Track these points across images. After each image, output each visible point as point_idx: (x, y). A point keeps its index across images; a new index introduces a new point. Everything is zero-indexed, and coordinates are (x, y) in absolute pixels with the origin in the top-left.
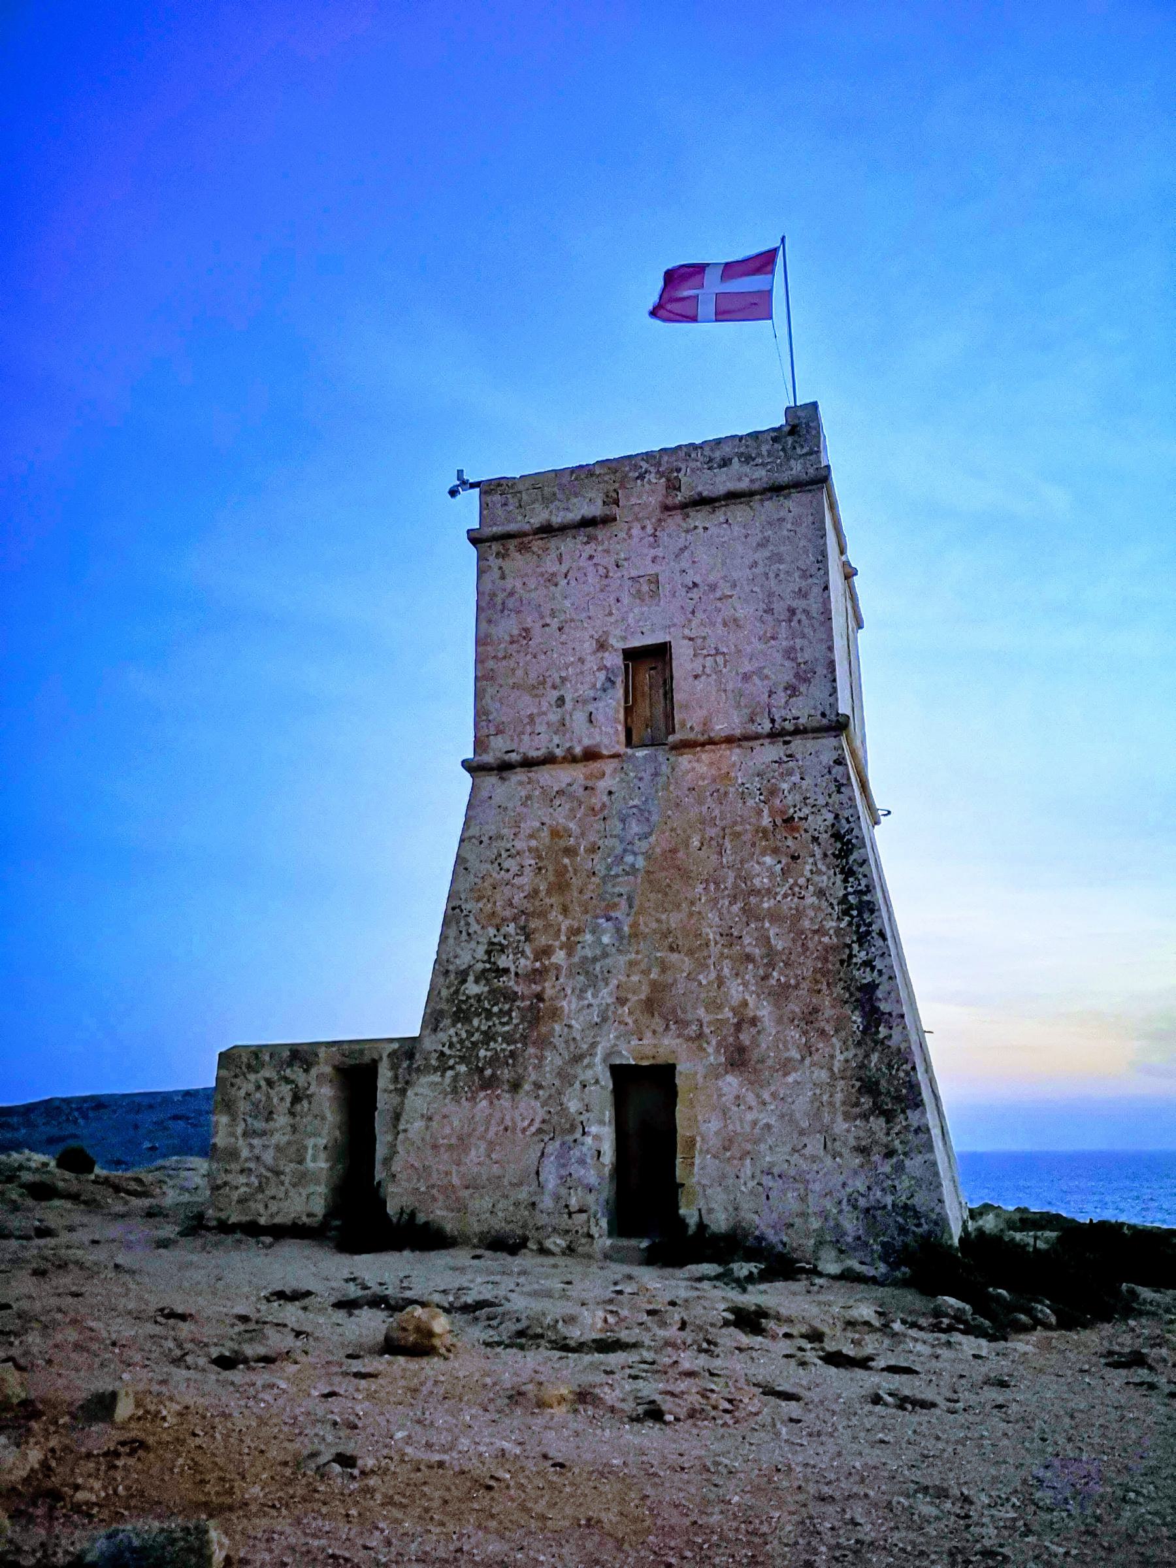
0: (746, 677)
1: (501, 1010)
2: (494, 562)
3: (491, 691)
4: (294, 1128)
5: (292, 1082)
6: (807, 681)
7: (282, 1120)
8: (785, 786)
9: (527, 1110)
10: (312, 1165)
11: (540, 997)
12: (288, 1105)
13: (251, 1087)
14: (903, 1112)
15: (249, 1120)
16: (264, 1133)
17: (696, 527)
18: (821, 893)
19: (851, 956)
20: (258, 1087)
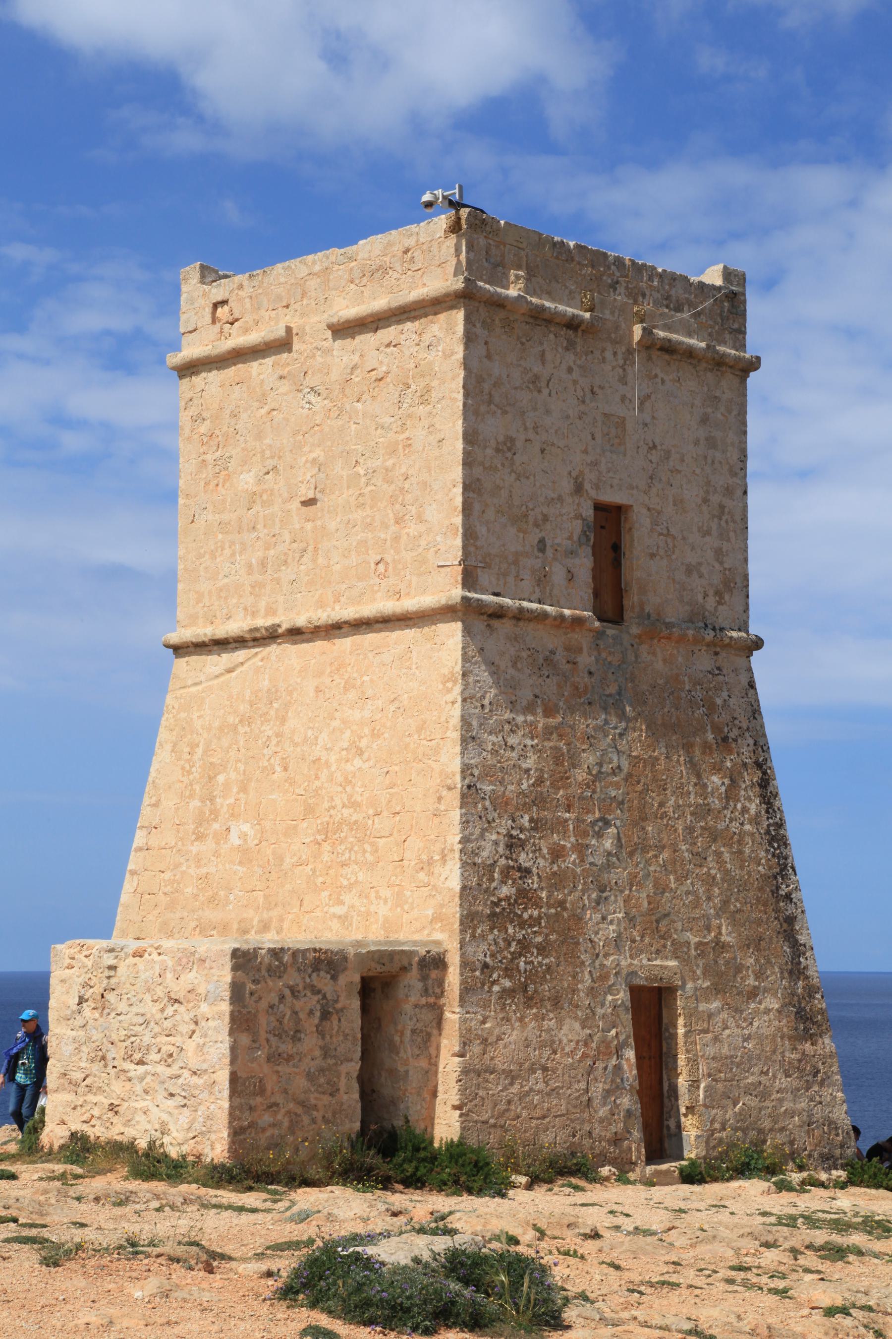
0: (689, 570)
1: (531, 917)
2: (478, 330)
3: (477, 507)
4: (326, 1052)
5: (319, 992)
6: (730, 590)
7: (310, 1042)
8: (719, 701)
9: (570, 1031)
10: (345, 1097)
11: (561, 904)
12: (316, 1021)
13: (274, 998)
14: (821, 1037)
15: (274, 1040)
16: (289, 1058)
17: (656, 376)
18: (755, 821)
19: (778, 888)
20: (282, 998)
